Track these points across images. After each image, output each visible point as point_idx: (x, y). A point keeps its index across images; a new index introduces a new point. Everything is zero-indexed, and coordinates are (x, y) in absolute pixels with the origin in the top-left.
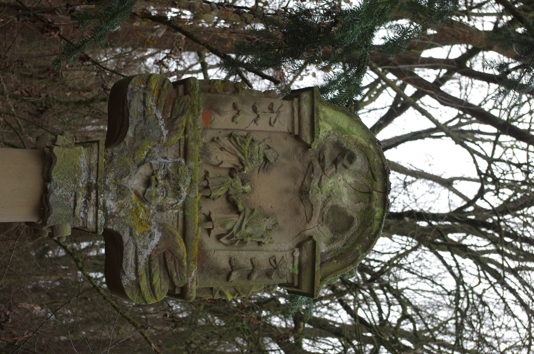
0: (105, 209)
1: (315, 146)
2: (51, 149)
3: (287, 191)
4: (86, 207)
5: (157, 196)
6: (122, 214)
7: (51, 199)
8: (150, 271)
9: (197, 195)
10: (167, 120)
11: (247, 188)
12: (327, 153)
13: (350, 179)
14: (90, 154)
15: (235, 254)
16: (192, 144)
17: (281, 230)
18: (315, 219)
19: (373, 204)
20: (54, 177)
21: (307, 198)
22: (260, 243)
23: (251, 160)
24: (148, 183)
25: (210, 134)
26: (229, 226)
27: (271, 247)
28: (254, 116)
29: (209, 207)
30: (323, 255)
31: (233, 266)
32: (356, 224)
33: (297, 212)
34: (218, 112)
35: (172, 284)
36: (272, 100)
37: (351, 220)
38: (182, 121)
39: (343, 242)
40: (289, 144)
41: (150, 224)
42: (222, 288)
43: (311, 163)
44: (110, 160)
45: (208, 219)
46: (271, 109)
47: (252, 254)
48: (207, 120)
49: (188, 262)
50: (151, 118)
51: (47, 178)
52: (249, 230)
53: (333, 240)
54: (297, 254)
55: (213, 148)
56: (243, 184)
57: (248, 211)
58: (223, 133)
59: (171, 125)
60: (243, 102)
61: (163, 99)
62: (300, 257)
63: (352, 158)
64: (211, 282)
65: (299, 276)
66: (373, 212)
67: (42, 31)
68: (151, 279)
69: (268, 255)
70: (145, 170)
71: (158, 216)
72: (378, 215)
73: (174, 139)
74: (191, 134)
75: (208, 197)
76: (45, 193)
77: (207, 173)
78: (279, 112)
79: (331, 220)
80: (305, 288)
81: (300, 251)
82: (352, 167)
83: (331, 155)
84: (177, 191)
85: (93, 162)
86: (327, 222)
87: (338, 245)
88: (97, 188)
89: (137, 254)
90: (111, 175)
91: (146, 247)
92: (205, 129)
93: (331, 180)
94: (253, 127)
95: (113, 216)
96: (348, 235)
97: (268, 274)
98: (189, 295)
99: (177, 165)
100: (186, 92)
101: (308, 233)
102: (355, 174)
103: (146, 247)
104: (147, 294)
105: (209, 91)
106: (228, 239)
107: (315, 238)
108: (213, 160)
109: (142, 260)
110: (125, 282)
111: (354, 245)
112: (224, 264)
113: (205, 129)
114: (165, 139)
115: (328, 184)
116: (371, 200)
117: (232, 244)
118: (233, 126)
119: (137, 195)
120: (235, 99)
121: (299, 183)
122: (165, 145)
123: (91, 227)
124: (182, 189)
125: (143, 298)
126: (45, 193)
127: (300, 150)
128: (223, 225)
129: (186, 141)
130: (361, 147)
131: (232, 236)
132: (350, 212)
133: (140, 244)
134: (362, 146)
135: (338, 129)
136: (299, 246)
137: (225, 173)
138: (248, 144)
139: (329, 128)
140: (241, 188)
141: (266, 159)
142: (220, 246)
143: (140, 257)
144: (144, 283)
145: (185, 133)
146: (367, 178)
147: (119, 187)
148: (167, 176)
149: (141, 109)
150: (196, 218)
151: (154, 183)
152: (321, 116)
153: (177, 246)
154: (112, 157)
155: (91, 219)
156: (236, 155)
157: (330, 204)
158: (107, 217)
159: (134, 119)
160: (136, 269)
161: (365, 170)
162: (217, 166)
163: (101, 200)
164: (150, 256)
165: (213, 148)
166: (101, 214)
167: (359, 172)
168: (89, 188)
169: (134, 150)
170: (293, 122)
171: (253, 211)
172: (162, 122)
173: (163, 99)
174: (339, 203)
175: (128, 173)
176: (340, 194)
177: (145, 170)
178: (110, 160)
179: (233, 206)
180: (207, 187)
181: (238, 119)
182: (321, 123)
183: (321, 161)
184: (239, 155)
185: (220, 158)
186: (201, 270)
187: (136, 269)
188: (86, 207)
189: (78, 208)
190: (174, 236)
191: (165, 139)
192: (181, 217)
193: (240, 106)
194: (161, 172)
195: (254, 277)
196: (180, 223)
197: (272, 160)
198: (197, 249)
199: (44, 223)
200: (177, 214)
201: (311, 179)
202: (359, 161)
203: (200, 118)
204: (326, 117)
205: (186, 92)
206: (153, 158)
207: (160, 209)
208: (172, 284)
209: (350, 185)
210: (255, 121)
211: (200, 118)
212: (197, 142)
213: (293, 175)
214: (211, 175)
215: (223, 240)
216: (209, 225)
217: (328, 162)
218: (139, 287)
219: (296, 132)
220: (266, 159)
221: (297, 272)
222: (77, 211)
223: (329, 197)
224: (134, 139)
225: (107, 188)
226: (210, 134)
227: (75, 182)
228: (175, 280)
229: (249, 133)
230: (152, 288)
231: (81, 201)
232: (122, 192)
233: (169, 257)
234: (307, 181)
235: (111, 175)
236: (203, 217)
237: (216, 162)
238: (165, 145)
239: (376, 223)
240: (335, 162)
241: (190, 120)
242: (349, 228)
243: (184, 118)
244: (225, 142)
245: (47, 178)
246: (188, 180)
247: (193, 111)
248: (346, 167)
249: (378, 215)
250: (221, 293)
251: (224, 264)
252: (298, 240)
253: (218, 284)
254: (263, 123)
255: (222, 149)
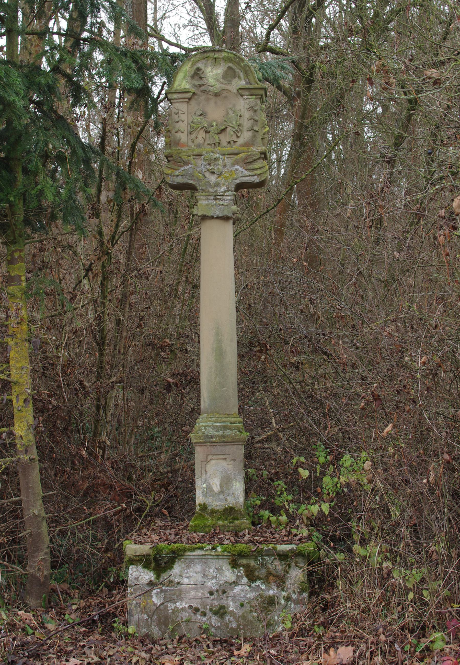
0: (225, 192)
1: (193, 90)
2: (199, 217)
3: (216, 103)
4: (224, 200)
5: (218, 169)
6: (227, 184)
7: (220, 215)
8: (253, 169)
9: (218, 149)
10: (184, 165)
11: (214, 124)
12: (197, 83)
13: (209, 69)
14: (201, 199)
15: (246, 128)
16: (195, 153)
17: (234, 106)
18: (229, 88)
19: (221, 57)
20: (211, 214)
21: (219, 93)
22: (240, 116)
23: (201, 123)
24: (213, 173)
25: (190, 143)
26: (232, 133)
27: (242, 110)
28: (181, 122)
29: (224, 143)
30: (246, 83)
31: (251, 129)
32: (231, 65)
33: (226, 97)
34: (179, 140)
35: (259, 159)
36: (173, 113)
37: (230, 68)
38: (185, 158)
39: (240, 71)
40: (193, 102)
41: (232, 171)
42: (261, 134)
43: (202, 91)
44: (203, 190)
45: (229, 142)
46: (177, 114)
47: (246, 120)
48: (183, 145)
49: (249, 152)
50: (184, 173)
51: (212, 217)
52: (234, 123)
53: (239, 77)
54: (245, 97)
55: (197, 142)
56: (213, 126)
57: (225, 123)
58: (189, 137)
59: (186, 163)
60: (174, 128)
61: (175, 167)
62: (247, 95)
63: (198, 69)
64: (259, 140)
65: (256, 95)
66: (224, 57)
67: (145, 214)
68: (257, 169)
69: (246, 112)
70: (207, 174)
71: (228, 167)
72: (226, 54)
73: (193, 161)
74: (190, 153)
75: (219, 143)
76: (218, 218)
77: (208, 144)
78: (178, 110)
79: (229, 79)
80: (262, 92)
81: (244, 95)
82: (203, 69)
83: (197, 80)
84: (216, 159)
85: (204, 198)
86: (230, 81)
87: (241, 75)
88: (215, 196)
89: (245, 176)
90: (210, 189)
91: (242, 172)
92: (188, 146)
93: (210, 80)
94: (186, 122)
95: (228, 188)
96: (236, 69)
97: (255, 111)
98: (264, 151)
99: (204, 160)
100: (172, 157)
101: (235, 91)
102: (206, 66)
103: (242, 172)
104: (264, 170)
105: (170, 144)
106: (238, 132)
107: (238, 88)
108: (202, 142)
109: (248, 173)
110: (258, 180)
111: (241, 67)
112: (250, 133)
113: (188, 146)
114: (193, 166)
115: (211, 81)
116: (219, 58)
117: (241, 130)
118: (186, 133)
119: (219, 177)
120: (173, 132)
121: (212, 97)
122: (196, 166)
123: (233, 197)
124: (215, 157)
125: (265, 172)
126: (218, 218)
127: (196, 97)
128: (232, 136)
129: (194, 155)
130: (193, 65)
131: (237, 131)
132: (225, 68)
133: (241, 175)
134: (192, 64)
135: (184, 78)
136: (242, 96)
137: (208, 135)
138: (194, 125)
139: (184, 83)
140: (214, 127)
141: (201, 115)
142: (242, 136)
143: (246, 175)
144: (258, 172)
145: (190, 156)
146: (208, 60)
147: (215, 186)
148: (209, 164)
149: (180, 177)
150: (229, 149)
151: (213, 170)
152: (179, 88)
153: (241, 158)
154: (202, 190)
155: (229, 198)
156: (199, 131)
157: (221, 80)
158: (228, 191)
159: (185, 180)
160: (252, 176)
161: (204, 61)
162: (205, 140)
163: (221, 194)
164: (246, 170)
165: (197, 142)
166: (227, 194)
167: (205, 64)
168: (216, 199)
169: (199, 180)
170: (182, 102)
171: (225, 121)
172: (186, 168)
173: (175, 167)
174: (221, 75)
175: (209, 182)
176: (217, 74)
177: (207, 174)
178: (203, 190)
179: (224, 130)
180: (215, 144)
181: (182, 130)
182: (182, 88)
183: (200, 86)
184: (199, 129)
185: (201, 139)
186: (253, 145)
187: (252, 176)
188: (224, 200)
189: (224, 204)
190: (237, 159)
191: (193, 166)
192: (228, 156)
193: (176, 130)
194: (208, 167)
195: (256, 118)
196: (231, 156)
197: (201, 112)
198: (243, 148)
199: (232, 217)
200: (227, 158)
201: (209, 91)
202: (200, 65)
203: (183, 149)
204: (179, 85)
205: (172, 157)
206: (202, 171)
207: (225, 166)
208: (259, 159)
209: (212, 69)
210: (183, 121)
211: (183, 149)
212: (194, 150)
213: (208, 100)
214: (209, 142)
215: (239, 135)
216: (232, 142)
217: (200, 82)
218: (260, 174)
219: (187, 100)
220: (201, 115)
221: (254, 97)
222: (226, 204)
223: (218, 80)
224: (194, 180)
225: (216, 191)
226: (190, 143)
227: (213, 205)
228: (257, 158)
229: (188, 124)
230: (261, 168)
231: (221, 203)
232: (217, 185)
233: (246, 161)
234: (211, 93)
235: (210, 189)
236: (229, 145)
237: (203, 140)
238: (196, 166)
239: (230, 55)
240: (201, 78)
241: (184, 154)
242: (233, 69)
243: (183, 157)
244: (193, 136)
245: (212, 217)
246: (212, 154)
247: (180, 153)
248: (203, 72)
249: (226, 54)
250: (264, 134)
251: (250, 133)
252: (239, 96)
253: (260, 135)
254: (184, 117)
255: (196, 138)
